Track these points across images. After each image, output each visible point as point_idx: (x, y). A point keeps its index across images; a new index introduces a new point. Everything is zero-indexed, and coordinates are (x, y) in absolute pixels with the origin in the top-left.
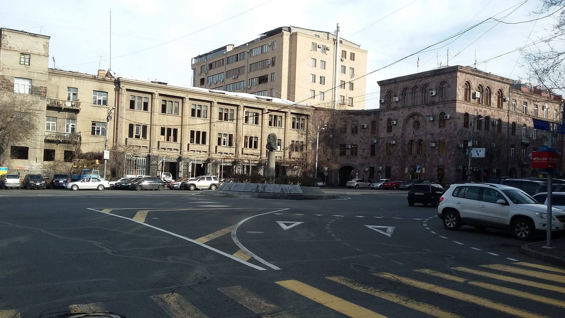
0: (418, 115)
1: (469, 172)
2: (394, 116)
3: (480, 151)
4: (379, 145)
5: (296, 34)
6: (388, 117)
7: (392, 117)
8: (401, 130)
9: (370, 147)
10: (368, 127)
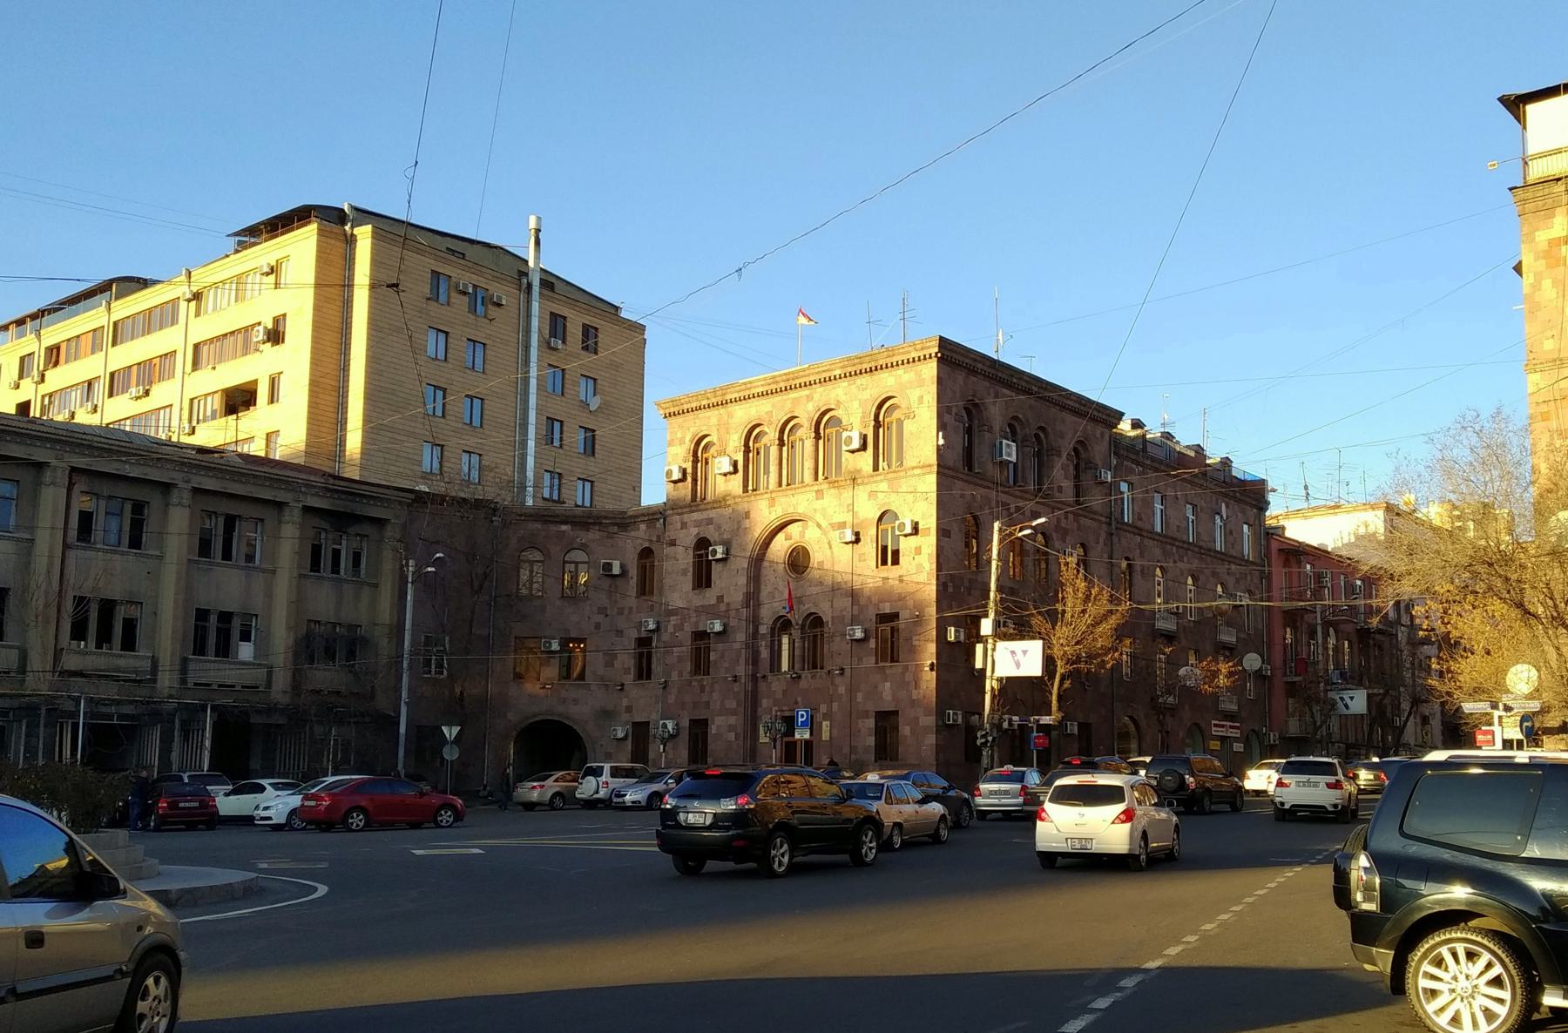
1: (987, 733)
2: (719, 527)
4: (665, 637)
6: (698, 534)
7: (711, 533)
10: (624, 573)
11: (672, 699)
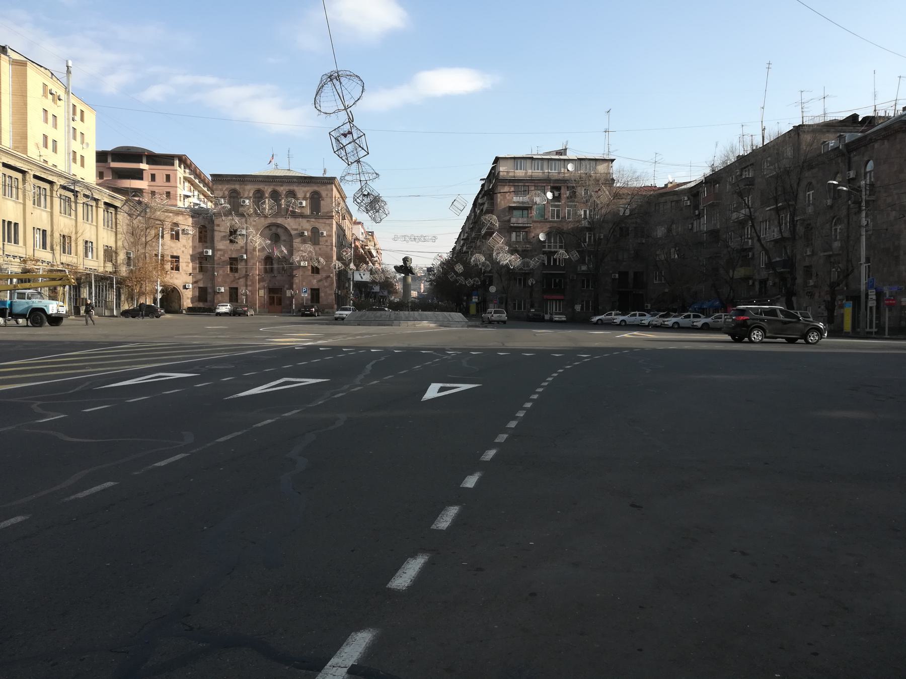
0: (278, 226)
3: (364, 274)
5: (23, 64)
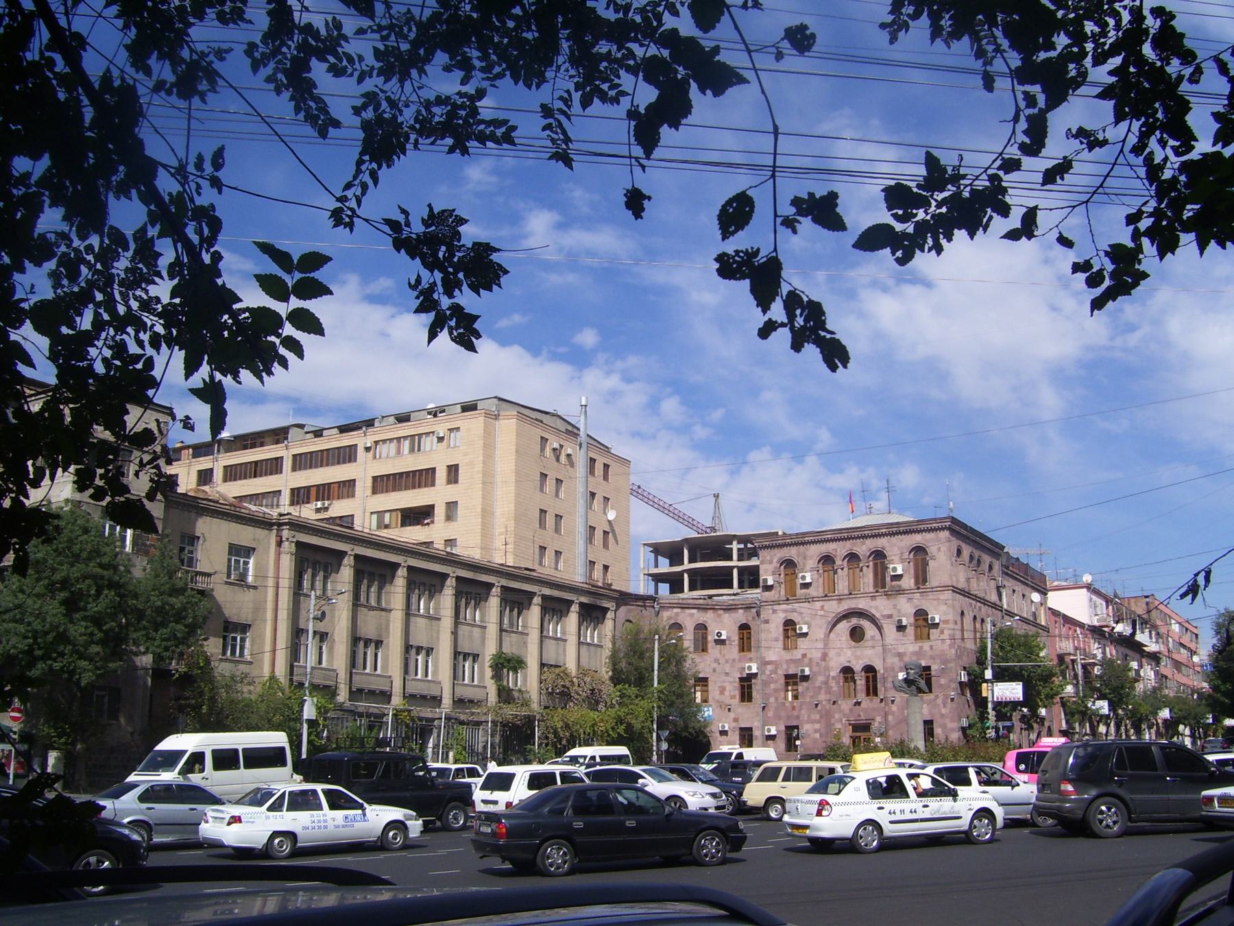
0: (861, 614)
7: (794, 617)
8: (821, 645)
9: (737, 684)
11: (771, 714)
